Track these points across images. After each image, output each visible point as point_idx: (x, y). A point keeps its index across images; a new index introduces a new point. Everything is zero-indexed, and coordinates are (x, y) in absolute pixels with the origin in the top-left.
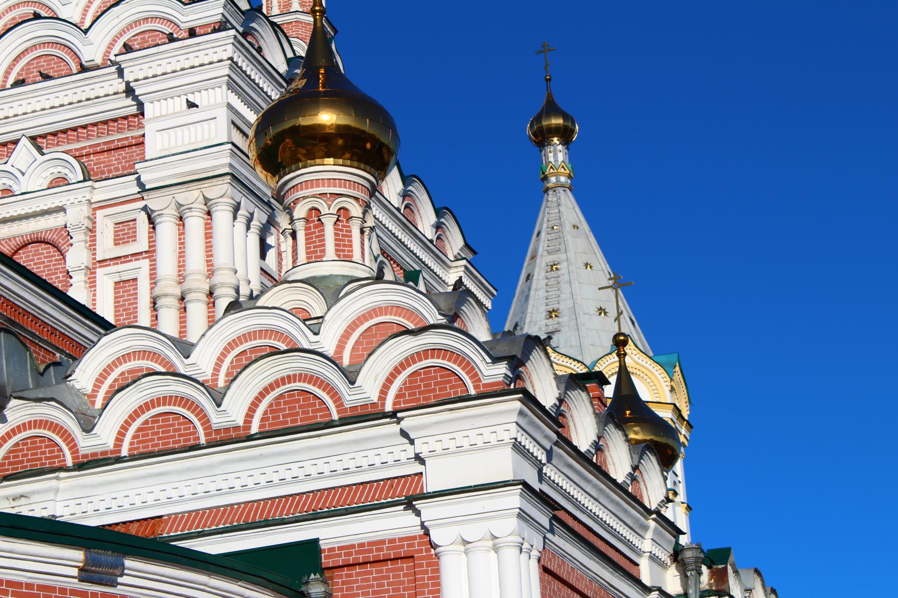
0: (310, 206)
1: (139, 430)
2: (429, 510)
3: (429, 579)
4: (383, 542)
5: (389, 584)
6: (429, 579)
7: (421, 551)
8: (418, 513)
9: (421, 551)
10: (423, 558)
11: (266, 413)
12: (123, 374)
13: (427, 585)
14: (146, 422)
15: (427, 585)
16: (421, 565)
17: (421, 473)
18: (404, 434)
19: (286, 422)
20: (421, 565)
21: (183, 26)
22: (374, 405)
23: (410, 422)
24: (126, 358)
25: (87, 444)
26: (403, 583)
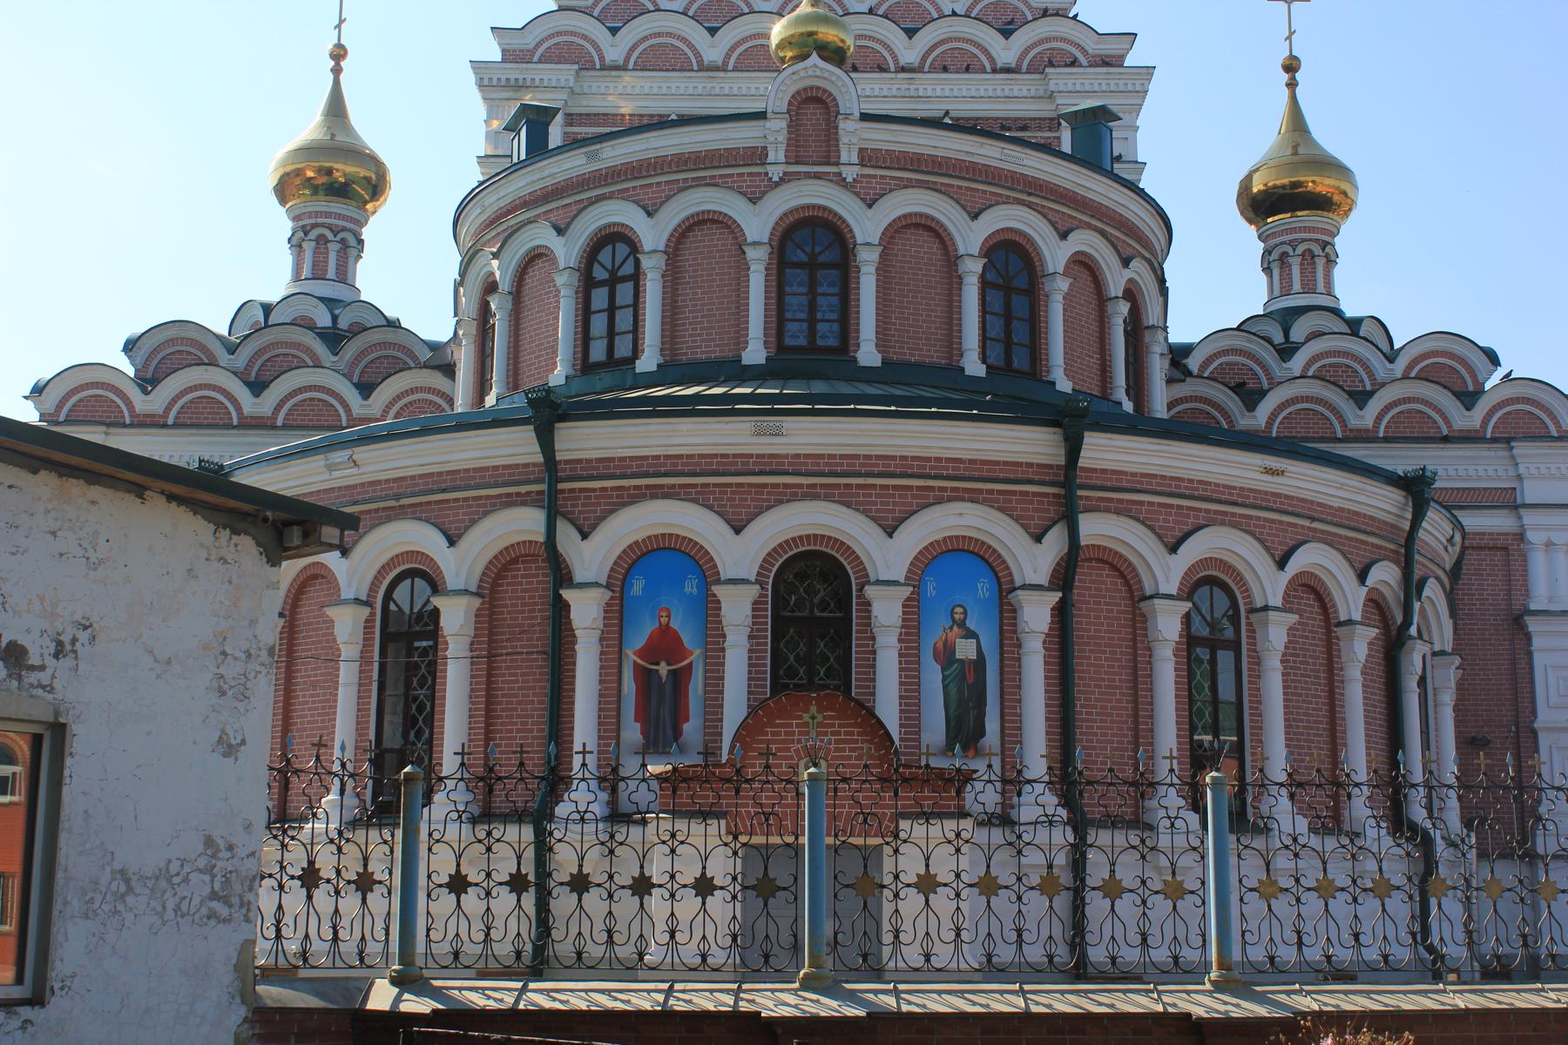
0: (1307, 247)
1: (1285, 418)
2: (1529, 518)
3: (1520, 566)
4: (1484, 534)
5: (1487, 565)
6: (1520, 566)
7: (1513, 545)
8: (1520, 518)
9: (1513, 545)
10: (1515, 550)
11: (1389, 422)
12: (1221, 364)
13: (1518, 570)
14: (1290, 413)
15: (1518, 570)
16: (1514, 555)
17: (1515, 489)
18: (1513, 457)
19: (1429, 432)
20: (1514, 555)
21: (1090, 51)
22: (1476, 431)
23: (1520, 449)
24: (1225, 352)
25: (1245, 421)
26: (1497, 565)
